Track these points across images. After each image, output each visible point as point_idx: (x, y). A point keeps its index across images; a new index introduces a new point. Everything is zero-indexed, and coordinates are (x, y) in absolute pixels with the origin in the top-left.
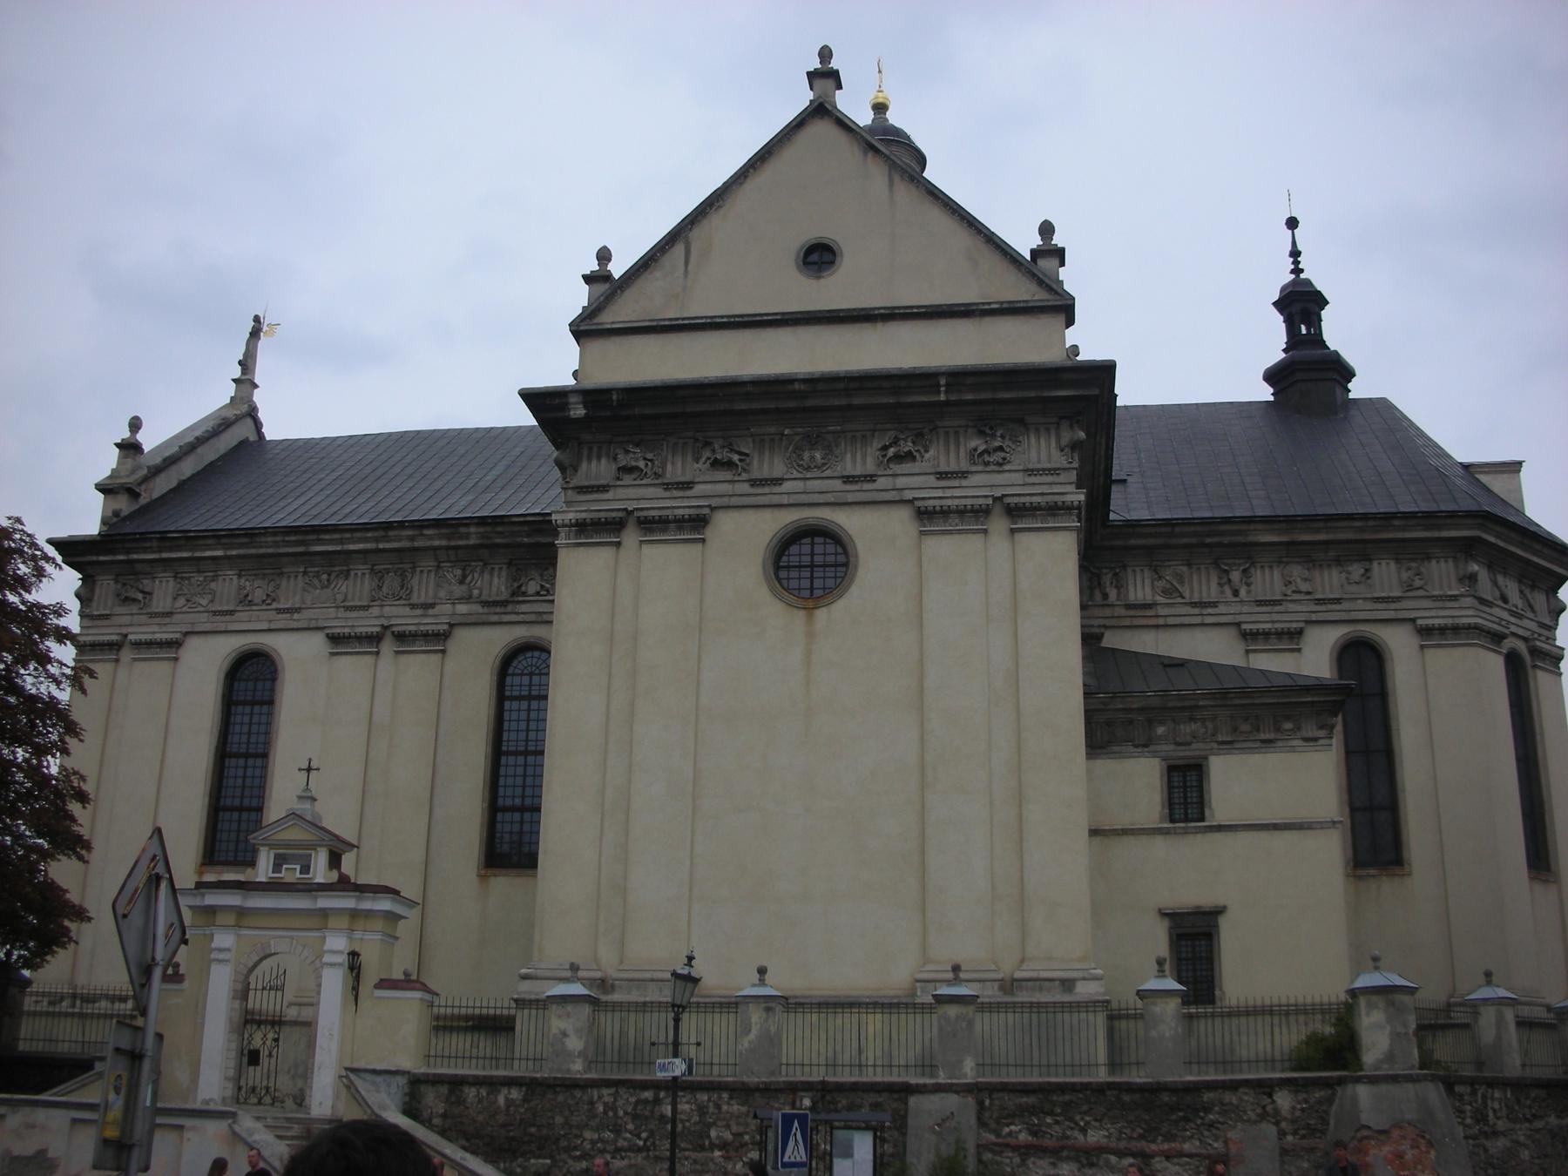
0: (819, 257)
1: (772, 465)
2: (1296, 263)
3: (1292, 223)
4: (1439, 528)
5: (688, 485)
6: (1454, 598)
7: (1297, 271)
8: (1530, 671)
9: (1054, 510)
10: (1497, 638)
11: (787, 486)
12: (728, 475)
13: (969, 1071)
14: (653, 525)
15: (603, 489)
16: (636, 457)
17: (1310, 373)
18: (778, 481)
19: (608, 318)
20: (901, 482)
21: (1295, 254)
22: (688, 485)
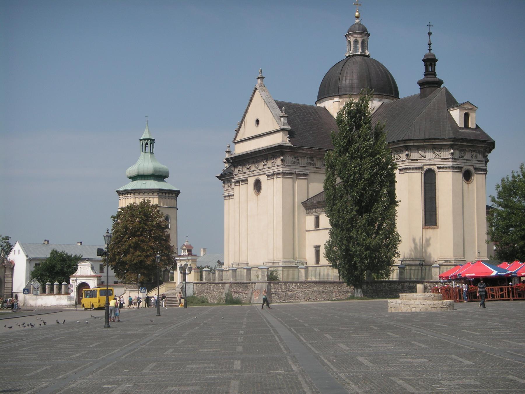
0: (257, 121)
1: (253, 168)
2: (430, 47)
3: (430, 34)
4: (398, 144)
5: (245, 173)
6: (405, 161)
7: (430, 50)
8: (437, 173)
9: (279, 174)
10: (419, 168)
11: (255, 172)
12: (248, 171)
13: (231, 280)
14: (242, 181)
15: (237, 175)
16: (239, 168)
17: (430, 83)
18: (253, 171)
19: (238, 139)
20: (266, 169)
21: (430, 44)
22: (245, 173)
